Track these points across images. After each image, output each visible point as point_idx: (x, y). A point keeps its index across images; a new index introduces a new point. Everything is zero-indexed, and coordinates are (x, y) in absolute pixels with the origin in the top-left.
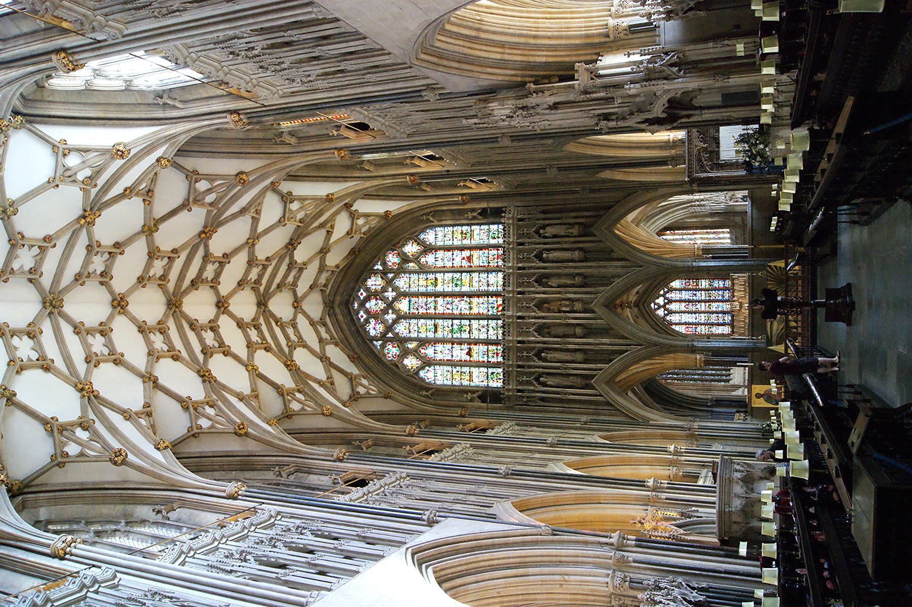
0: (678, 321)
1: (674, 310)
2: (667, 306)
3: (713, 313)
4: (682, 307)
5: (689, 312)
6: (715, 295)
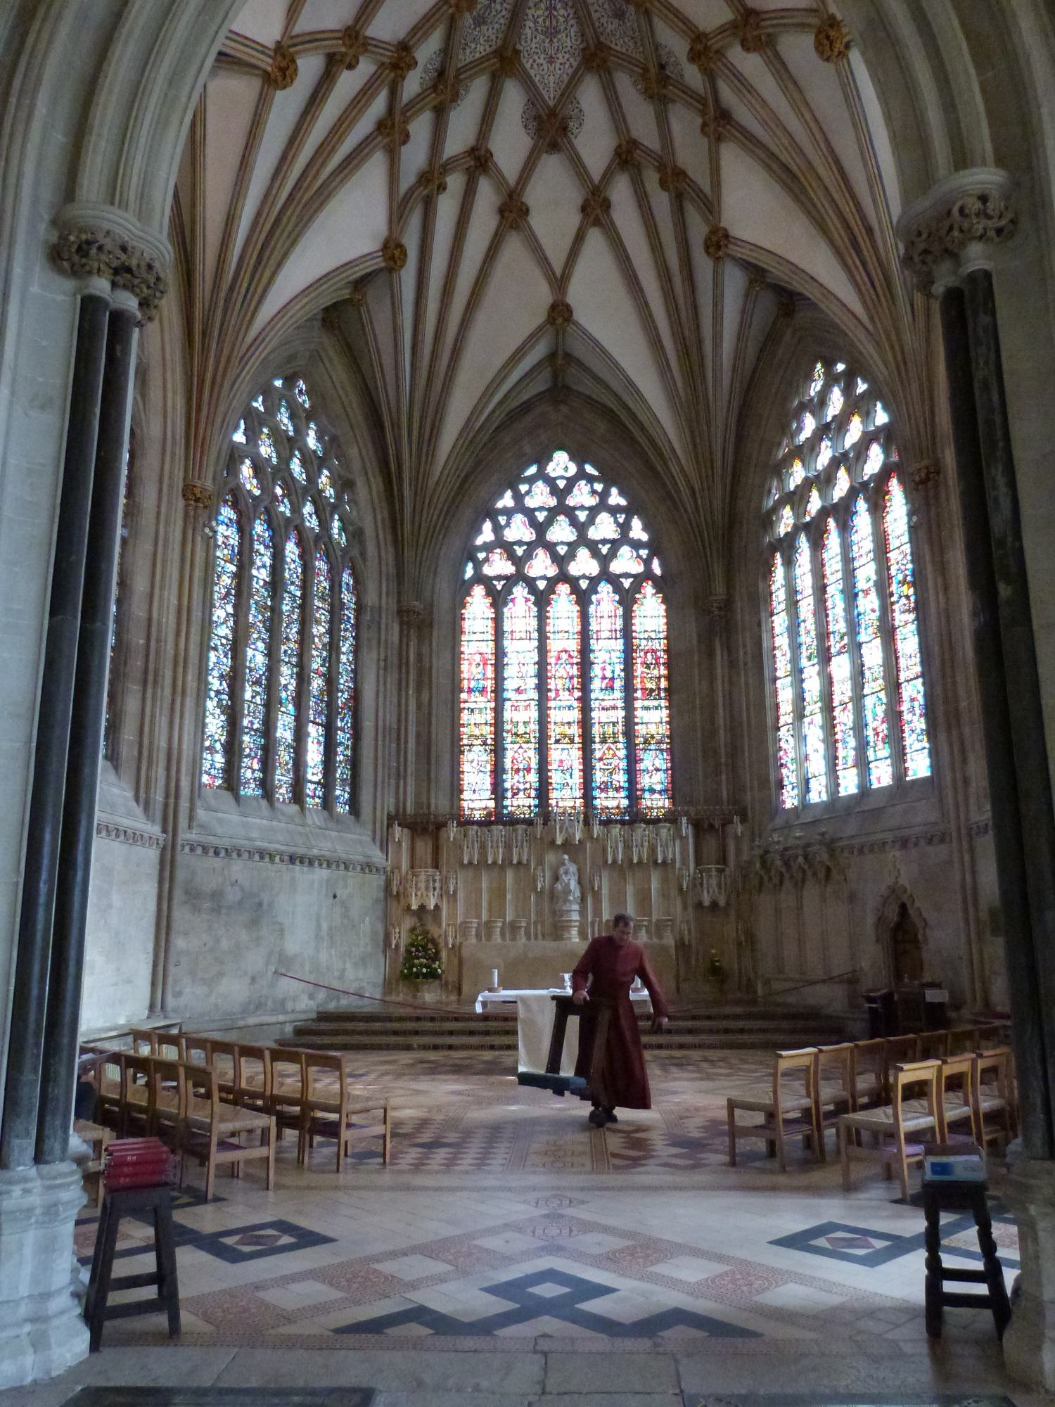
0: (507, 626)
1: (552, 611)
2: (564, 589)
3: (543, 750)
4: (564, 641)
5: (542, 665)
6: (610, 759)
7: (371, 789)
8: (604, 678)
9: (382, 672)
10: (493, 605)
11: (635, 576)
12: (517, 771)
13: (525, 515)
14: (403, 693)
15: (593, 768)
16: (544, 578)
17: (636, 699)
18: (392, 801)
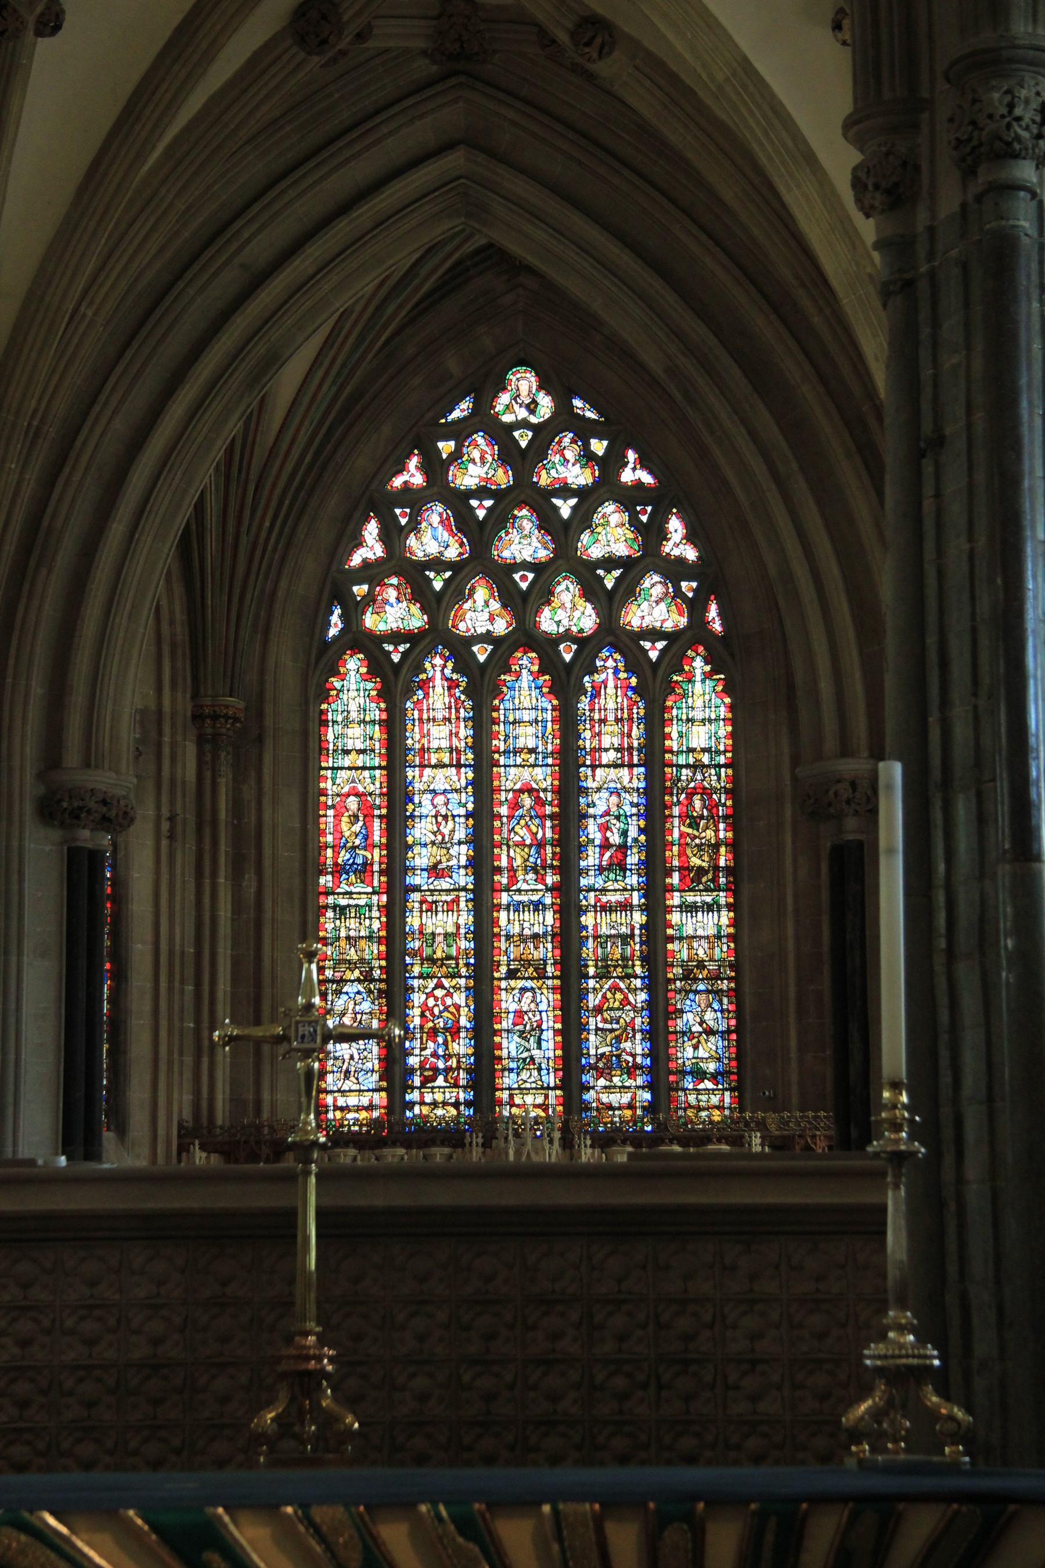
0: (413, 738)
1: (504, 709)
2: (526, 662)
7: (147, 1078)
8: (605, 845)
9: (164, 843)
10: (385, 694)
11: (672, 637)
12: (433, 1033)
13: (448, 505)
14: (207, 881)
15: (583, 1028)
16: (487, 637)
17: (671, 889)
18: (188, 1098)
